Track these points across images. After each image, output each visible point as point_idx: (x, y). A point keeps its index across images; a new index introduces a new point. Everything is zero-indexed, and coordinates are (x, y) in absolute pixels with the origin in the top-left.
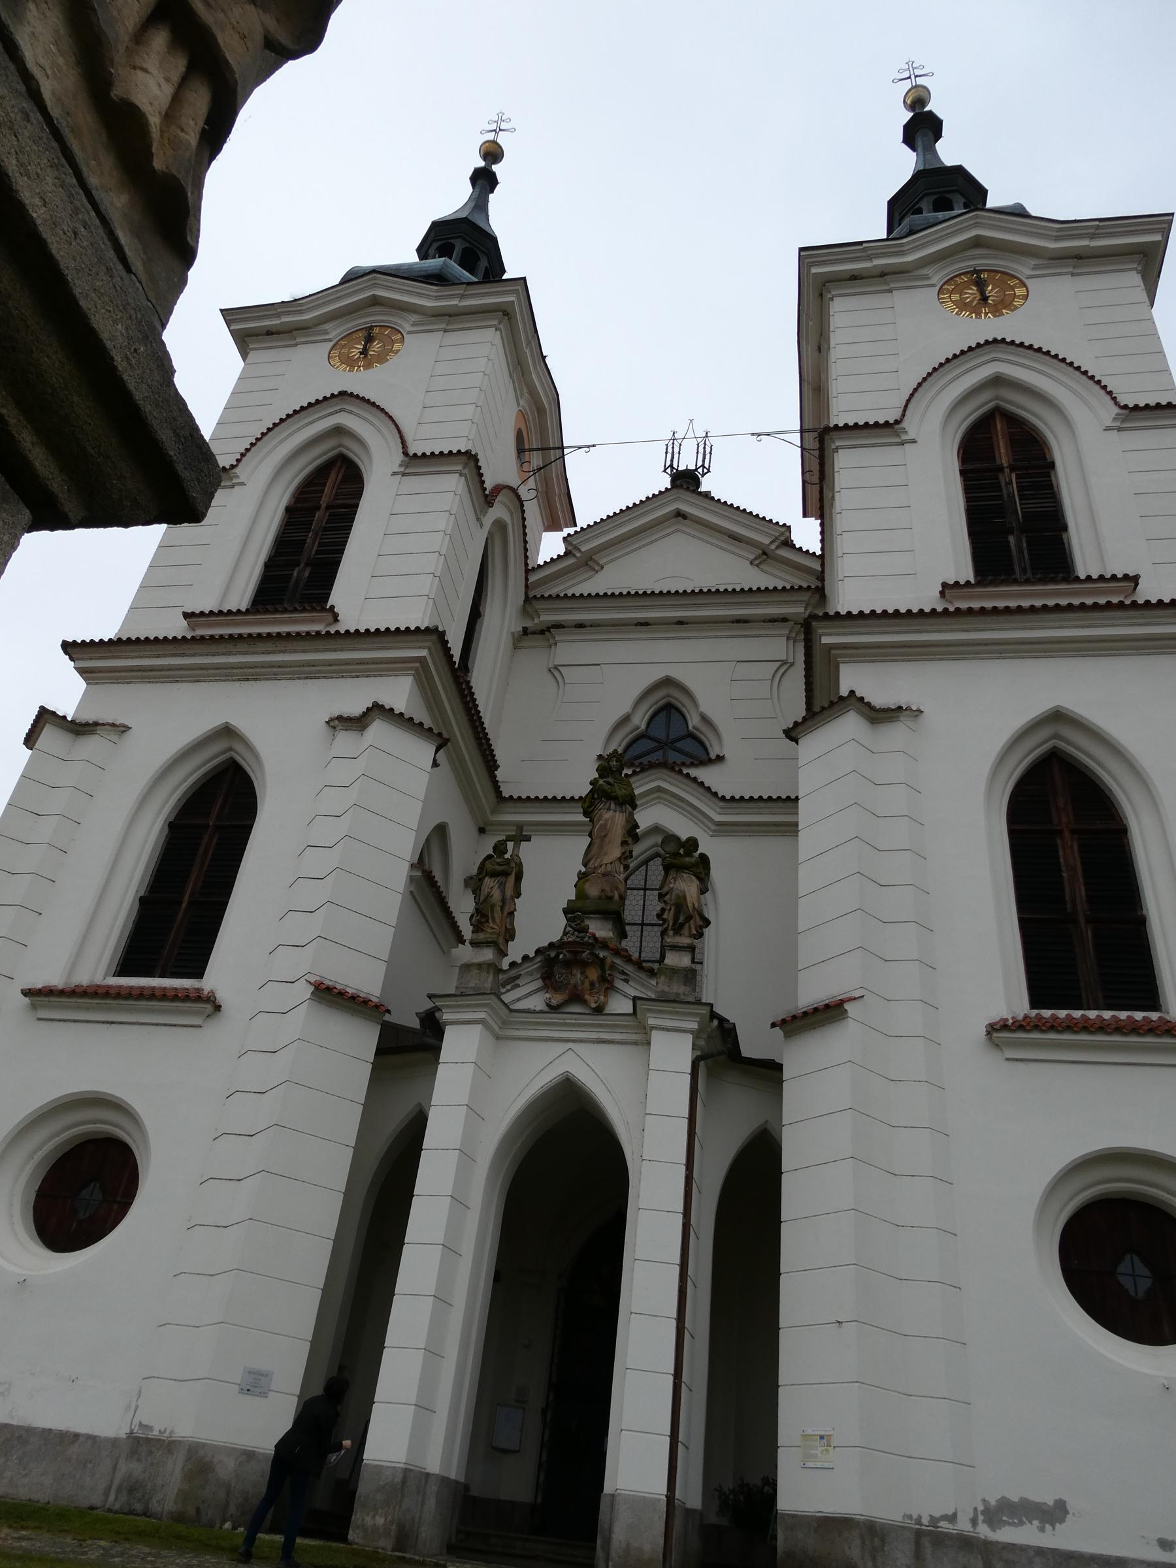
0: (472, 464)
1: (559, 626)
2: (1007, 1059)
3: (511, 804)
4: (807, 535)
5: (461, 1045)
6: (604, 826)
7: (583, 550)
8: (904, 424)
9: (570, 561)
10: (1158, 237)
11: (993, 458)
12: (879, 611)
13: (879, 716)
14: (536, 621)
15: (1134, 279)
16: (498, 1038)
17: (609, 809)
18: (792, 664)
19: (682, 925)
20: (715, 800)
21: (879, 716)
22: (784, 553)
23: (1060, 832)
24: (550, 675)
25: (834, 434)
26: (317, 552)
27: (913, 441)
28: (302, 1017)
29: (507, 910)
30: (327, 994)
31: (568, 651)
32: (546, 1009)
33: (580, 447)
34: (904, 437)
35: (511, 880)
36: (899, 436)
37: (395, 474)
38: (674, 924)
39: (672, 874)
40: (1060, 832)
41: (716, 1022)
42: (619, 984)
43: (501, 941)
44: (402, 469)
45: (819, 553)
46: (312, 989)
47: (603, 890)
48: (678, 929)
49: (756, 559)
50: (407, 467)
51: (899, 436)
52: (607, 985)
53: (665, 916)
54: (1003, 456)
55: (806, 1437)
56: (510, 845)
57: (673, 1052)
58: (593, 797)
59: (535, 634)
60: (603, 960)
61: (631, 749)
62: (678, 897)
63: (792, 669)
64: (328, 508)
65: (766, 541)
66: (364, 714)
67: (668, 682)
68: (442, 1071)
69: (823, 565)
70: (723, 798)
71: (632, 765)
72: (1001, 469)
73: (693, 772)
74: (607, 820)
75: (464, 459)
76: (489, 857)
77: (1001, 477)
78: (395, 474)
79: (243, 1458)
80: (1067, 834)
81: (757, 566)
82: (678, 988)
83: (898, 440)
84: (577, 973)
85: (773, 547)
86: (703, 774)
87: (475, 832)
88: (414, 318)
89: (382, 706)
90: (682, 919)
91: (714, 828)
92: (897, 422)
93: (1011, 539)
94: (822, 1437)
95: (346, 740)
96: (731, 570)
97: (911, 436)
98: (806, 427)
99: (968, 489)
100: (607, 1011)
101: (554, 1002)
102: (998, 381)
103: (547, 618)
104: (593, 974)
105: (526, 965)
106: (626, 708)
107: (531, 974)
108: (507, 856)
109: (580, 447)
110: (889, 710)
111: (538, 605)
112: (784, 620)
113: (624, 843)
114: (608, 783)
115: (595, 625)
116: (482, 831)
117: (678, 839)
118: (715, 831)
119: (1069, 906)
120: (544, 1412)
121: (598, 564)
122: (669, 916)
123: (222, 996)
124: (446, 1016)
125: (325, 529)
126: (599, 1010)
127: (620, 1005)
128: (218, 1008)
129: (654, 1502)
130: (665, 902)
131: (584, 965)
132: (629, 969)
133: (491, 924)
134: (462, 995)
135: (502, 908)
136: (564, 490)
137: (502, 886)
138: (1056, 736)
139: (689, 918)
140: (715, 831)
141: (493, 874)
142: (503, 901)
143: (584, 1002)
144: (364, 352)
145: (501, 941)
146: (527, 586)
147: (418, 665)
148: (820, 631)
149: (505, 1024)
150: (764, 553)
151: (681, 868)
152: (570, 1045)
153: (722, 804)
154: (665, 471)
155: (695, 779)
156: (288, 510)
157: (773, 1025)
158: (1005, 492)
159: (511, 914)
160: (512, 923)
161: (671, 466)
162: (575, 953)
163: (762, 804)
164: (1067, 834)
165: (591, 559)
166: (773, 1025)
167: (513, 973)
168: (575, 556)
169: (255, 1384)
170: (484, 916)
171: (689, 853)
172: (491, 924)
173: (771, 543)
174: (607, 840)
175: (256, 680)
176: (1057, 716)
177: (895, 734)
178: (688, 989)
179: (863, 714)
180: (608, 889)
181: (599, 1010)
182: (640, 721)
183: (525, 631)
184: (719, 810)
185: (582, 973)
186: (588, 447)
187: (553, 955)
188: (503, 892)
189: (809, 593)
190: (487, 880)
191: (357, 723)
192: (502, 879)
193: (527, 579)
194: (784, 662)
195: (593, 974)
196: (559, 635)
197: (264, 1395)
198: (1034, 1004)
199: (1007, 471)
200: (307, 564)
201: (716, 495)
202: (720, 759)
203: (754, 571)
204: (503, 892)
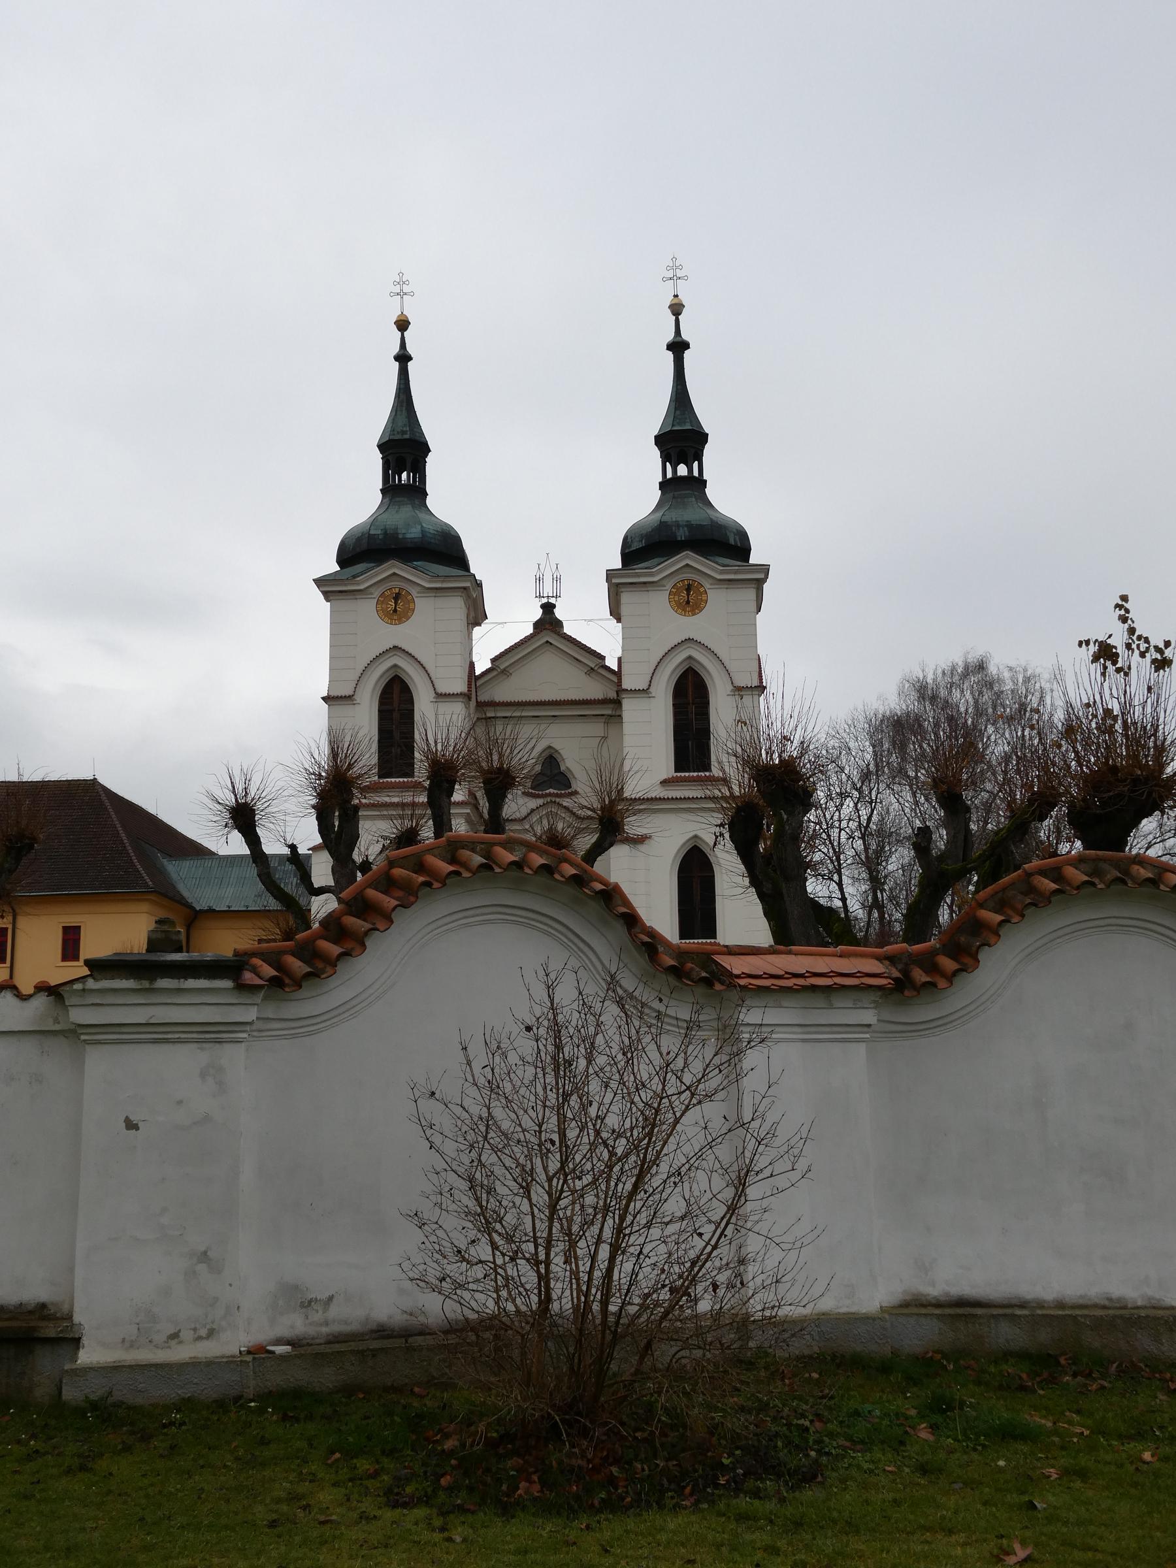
8: (651, 690)
9: (495, 673)
10: (762, 576)
15: (751, 594)
88: (419, 589)
99: (676, 714)
102: (690, 658)
144: (395, 611)
176: (696, 836)
201: (568, 630)
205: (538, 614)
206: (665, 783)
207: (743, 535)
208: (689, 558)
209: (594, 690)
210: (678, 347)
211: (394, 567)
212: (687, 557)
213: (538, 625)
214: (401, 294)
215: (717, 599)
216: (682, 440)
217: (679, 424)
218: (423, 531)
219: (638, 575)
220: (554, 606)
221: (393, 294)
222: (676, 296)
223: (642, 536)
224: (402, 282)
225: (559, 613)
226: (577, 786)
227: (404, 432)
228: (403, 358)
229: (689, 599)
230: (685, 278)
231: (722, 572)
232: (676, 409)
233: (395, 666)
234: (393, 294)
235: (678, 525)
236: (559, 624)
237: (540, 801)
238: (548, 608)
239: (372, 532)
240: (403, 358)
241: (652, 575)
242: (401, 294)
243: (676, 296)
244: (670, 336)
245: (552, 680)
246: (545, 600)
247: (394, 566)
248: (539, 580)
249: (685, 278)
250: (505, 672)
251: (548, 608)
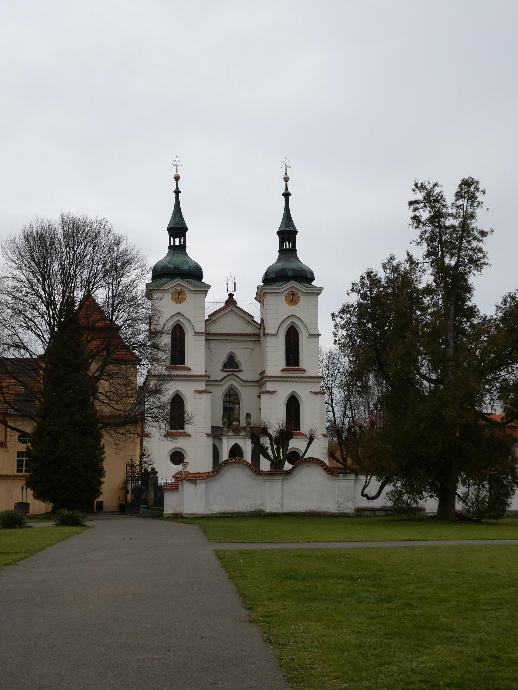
5: (225, 441)
13: (272, 393)
21: (272, 393)
28: (205, 438)
31: (212, 345)
52: (240, 432)
84: (237, 431)
88: (188, 290)
99: (286, 344)
102: (293, 322)
127: (241, 434)
144: (178, 298)
155: (238, 377)
177: (274, 396)
196: (210, 341)
201: (239, 305)
202: (241, 371)
205: (227, 298)
206: (283, 370)
207: (312, 274)
208: (293, 284)
209: (249, 330)
210: (287, 195)
211: (178, 281)
212: (293, 283)
213: (227, 302)
214: (177, 165)
215: (303, 300)
216: (287, 234)
217: (288, 227)
218: (190, 267)
219: (274, 289)
220: (233, 295)
221: (173, 165)
222: (286, 174)
223: (274, 273)
224: (177, 161)
225: (235, 298)
226: (243, 367)
227: (179, 224)
228: (177, 192)
229: (293, 299)
230: (290, 167)
231: (306, 290)
232: (286, 221)
233: (178, 320)
234: (173, 165)
235: (289, 270)
236: (235, 303)
237: (227, 374)
238: (231, 296)
239: (169, 266)
240: (177, 192)
241: (280, 289)
242: (177, 165)
243: (286, 174)
244: (283, 190)
245: (230, 325)
246: (229, 293)
247: (178, 281)
249: (290, 167)
250: (215, 321)
251: (231, 296)
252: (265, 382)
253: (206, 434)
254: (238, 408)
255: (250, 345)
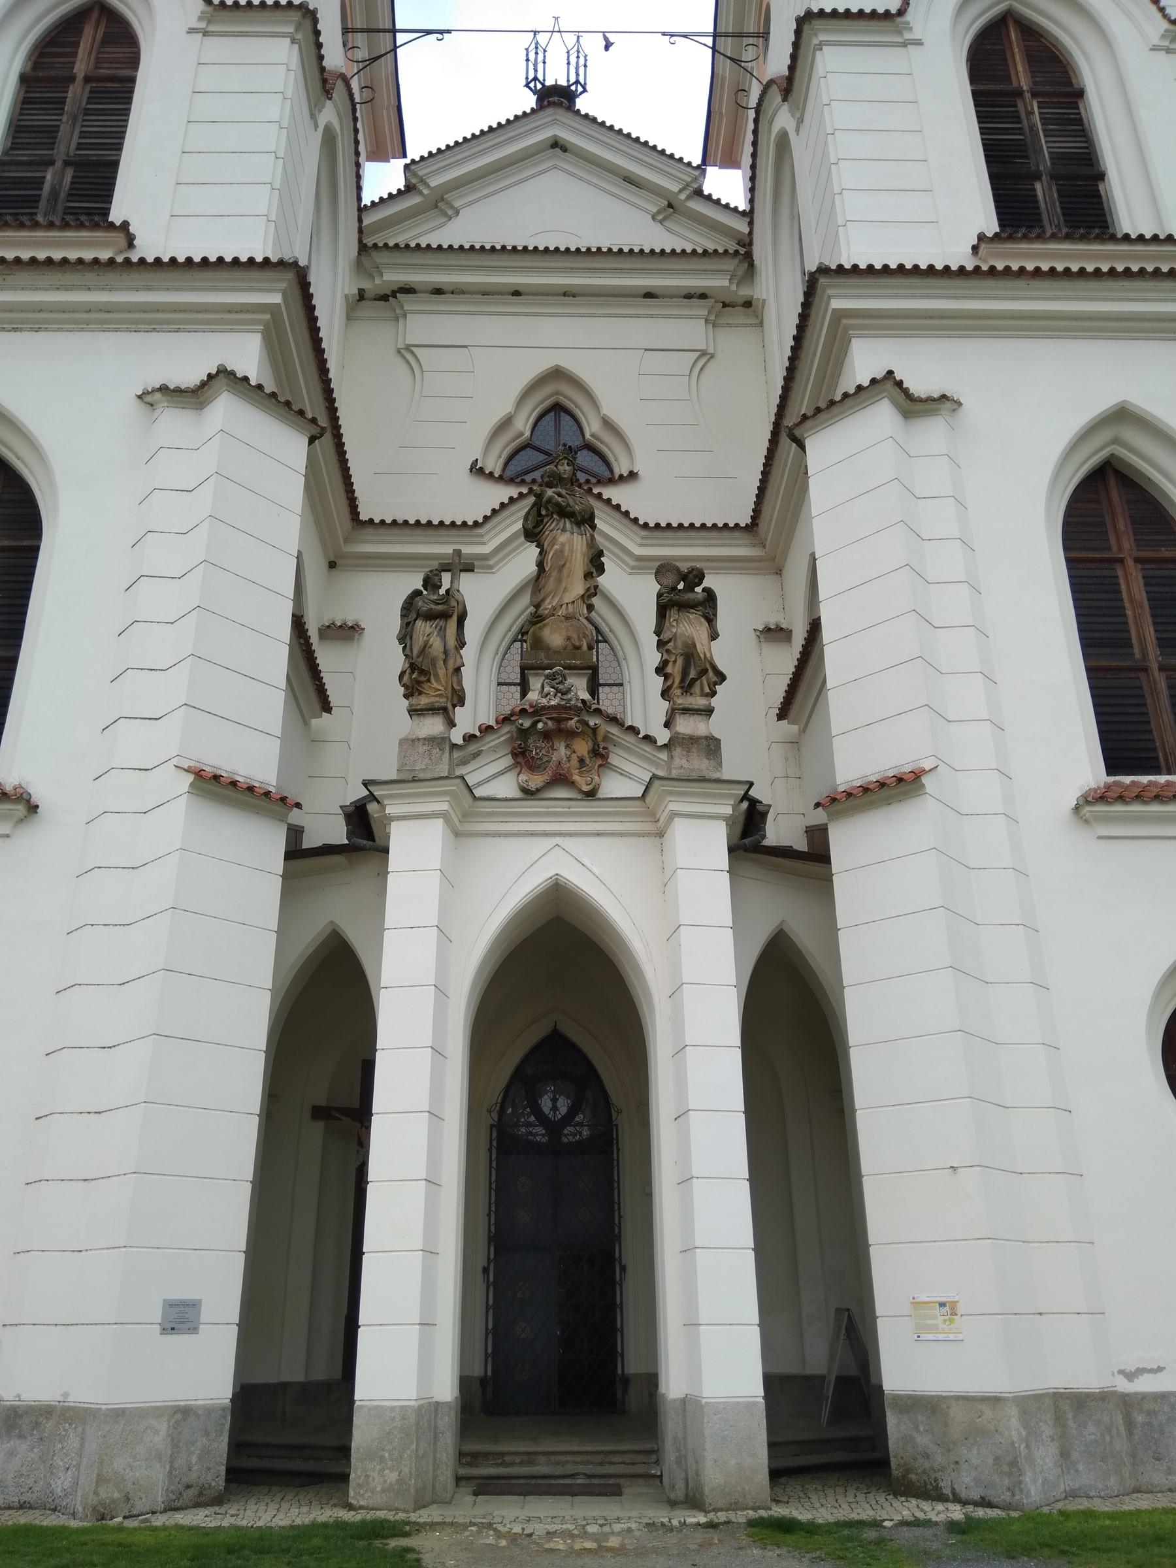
0: (308, 23)
1: (408, 290)
2: (1100, 838)
3: (370, 530)
4: (727, 185)
5: (416, 846)
6: (561, 552)
7: (432, 184)
8: (909, 17)
9: (413, 201)
11: (1007, 79)
12: (908, 266)
13: (914, 407)
14: (377, 281)
16: (457, 834)
17: (564, 530)
18: (712, 356)
19: (693, 681)
20: (635, 528)
21: (914, 407)
22: (696, 205)
23: (1121, 561)
24: (399, 359)
25: (817, 24)
26: (80, 147)
27: (918, 43)
29: (451, 664)
30: (212, 785)
31: (423, 325)
32: (519, 794)
33: (428, 32)
34: (908, 36)
35: (452, 624)
36: (900, 33)
37: (192, 31)
38: (683, 680)
39: (673, 615)
40: (1121, 561)
41: (745, 805)
42: (613, 760)
43: (450, 707)
44: (203, 25)
45: (742, 206)
46: (190, 778)
47: (569, 638)
48: (687, 687)
49: (659, 212)
50: (209, 22)
51: (900, 33)
53: (669, 669)
54: (1022, 77)
55: (916, 1304)
56: (446, 578)
57: (701, 844)
58: (539, 514)
59: (380, 301)
60: (594, 730)
61: (514, 462)
62: (685, 644)
63: (712, 362)
64: (87, 80)
65: (674, 187)
66: (203, 384)
67: (557, 374)
68: (395, 884)
69: (751, 224)
70: (646, 525)
71: (523, 482)
72: (1019, 93)
73: (607, 492)
74: (563, 545)
75: (296, 16)
76: (417, 593)
77: (1020, 103)
78: (192, 31)
79: (179, 1416)
80: (1130, 562)
81: (661, 222)
82: (699, 764)
83: (899, 40)
85: (683, 196)
86: (613, 493)
87: (324, 566)
89: (232, 373)
90: (693, 674)
91: (633, 563)
92: (901, 12)
93: (1038, 186)
94: (942, 1305)
95: (173, 423)
96: (630, 226)
97: (916, 34)
98: (722, 29)
100: (600, 795)
101: (533, 786)
103: (394, 277)
104: (582, 747)
105: (489, 738)
106: (507, 408)
107: (494, 749)
108: (442, 591)
109: (428, 32)
110: (930, 400)
111: (381, 258)
112: (703, 296)
113: (588, 576)
114: (559, 495)
115: (458, 291)
116: (332, 565)
117: (678, 569)
118: (633, 568)
119: (1136, 650)
120: (486, 1270)
121: (452, 207)
122: (675, 669)
123: (38, 794)
124: (391, 809)
125: (87, 112)
126: (591, 794)
128: (33, 809)
129: (750, 1406)
130: (668, 651)
131: (570, 735)
132: (630, 739)
133: (435, 685)
134: (414, 780)
135: (445, 661)
136: (394, 102)
137: (442, 632)
138: (1116, 441)
139: (704, 672)
140: (633, 568)
141: (430, 617)
142: (445, 652)
143: (572, 784)
145: (450, 707)
146: (360, 231)
147: (268, 316)
148: (830, 291)
149: (466, 816)
150: (670, 206)
151: (685, 606)
152: (558, 840)
153: (644, 533)
154: (527, 85)
156: (24, 79)
157: (818, 805)
158: (1025, 123)
159: (458, 670)
160: (460, 682)
161: (535, 79)
162: (558, 721)
163: (692, 534)
164: (1130, 562)
165: (443, 199)
166: (818, 805)
167: (473, 748)
168: (421, 193)
169: (181, 1318)
170: (422, 672)
171: (690, 588)
172: (435, 685)
173: (681, 191)
174: (565, 571)
175: (15, 330)
178: (713, 763)
179: (896, 404)
180: (575, 636)
181: (591, 794)
182: (523, 425)
183: (362, 295)
184: (639, 540)
185: (567, 746)
186: (441, 32)
187: (527, 723)
188: (444, 638)
189: (736, 261)
190: (419, 623)
191: (194, 396)
192: (442, 623)
193: (360, 221)
194: (703, 353)
195: (582, 747)
197: (194, 1330)
198: (1111, 769)
199: (1027, 95)
200: (67, 163)
202: (633, 475)
203: (656, 228)
204: (444, 638)
248: (536, 54)
252: (842, 331)
253: (199, 774)
254: (578, 564)
255: (689, 330)
